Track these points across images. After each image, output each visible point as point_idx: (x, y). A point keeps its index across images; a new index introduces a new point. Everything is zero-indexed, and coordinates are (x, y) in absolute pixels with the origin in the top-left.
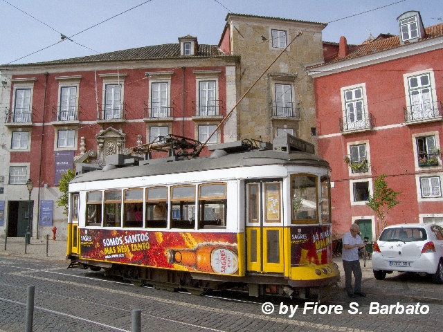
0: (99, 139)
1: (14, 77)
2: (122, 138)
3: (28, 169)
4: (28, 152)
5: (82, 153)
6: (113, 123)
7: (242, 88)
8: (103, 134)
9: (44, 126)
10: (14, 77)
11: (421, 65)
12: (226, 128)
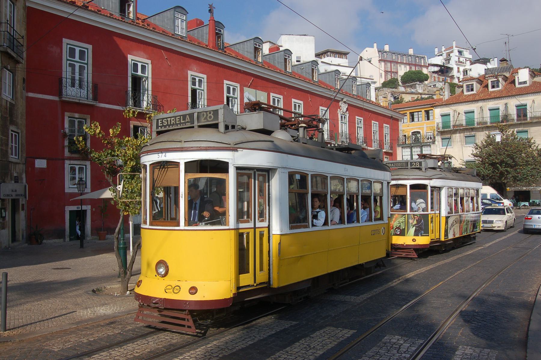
11: (142, 53)
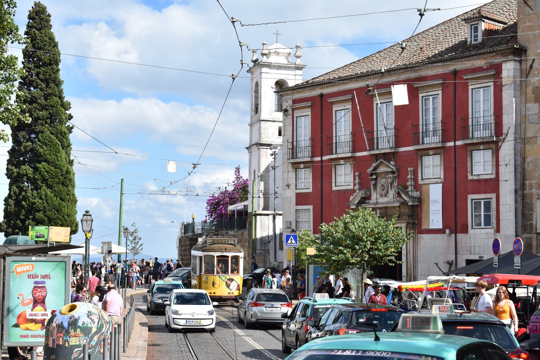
0: (372, 175)
1: (295, 102)
2: (393, 172)
3: (312, 210)
4: (310, 192)
5: (357, 191)
6: (385, 154)
7: (530, 89)
8: (376, 168)
9: (322, 161)
10: (295, 102)
12: (502, 153)
